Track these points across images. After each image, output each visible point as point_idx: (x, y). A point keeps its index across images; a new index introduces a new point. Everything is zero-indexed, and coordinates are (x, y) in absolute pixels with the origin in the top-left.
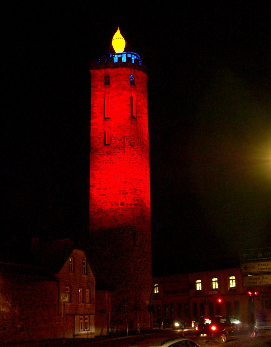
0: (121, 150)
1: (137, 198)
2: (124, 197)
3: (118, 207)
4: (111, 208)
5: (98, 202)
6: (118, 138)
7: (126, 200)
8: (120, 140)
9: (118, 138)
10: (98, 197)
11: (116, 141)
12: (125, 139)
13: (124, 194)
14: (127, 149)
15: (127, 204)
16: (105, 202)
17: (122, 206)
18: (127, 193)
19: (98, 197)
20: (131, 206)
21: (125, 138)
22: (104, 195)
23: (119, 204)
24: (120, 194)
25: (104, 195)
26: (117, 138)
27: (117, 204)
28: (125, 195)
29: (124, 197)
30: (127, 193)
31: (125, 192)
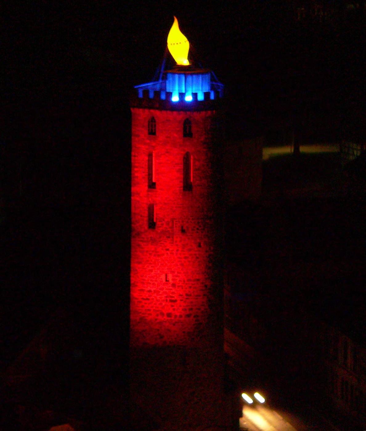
0: (169, 239)
2: (172, 306)
3: (164, 319)
4: (156, 320)
7: (174, 309)
10: (141, 302)
11: (162, 224)
13: (171, 301)
15: (176, 316)
16: (149, 310)
17: (169, 318)
19: (141, 302)
22: (148, 299)
24: (167, 300)
25: (148, 299)
26: (164, 220)
27: (162, 314)
29: (172, 306)
30: (176, 301)
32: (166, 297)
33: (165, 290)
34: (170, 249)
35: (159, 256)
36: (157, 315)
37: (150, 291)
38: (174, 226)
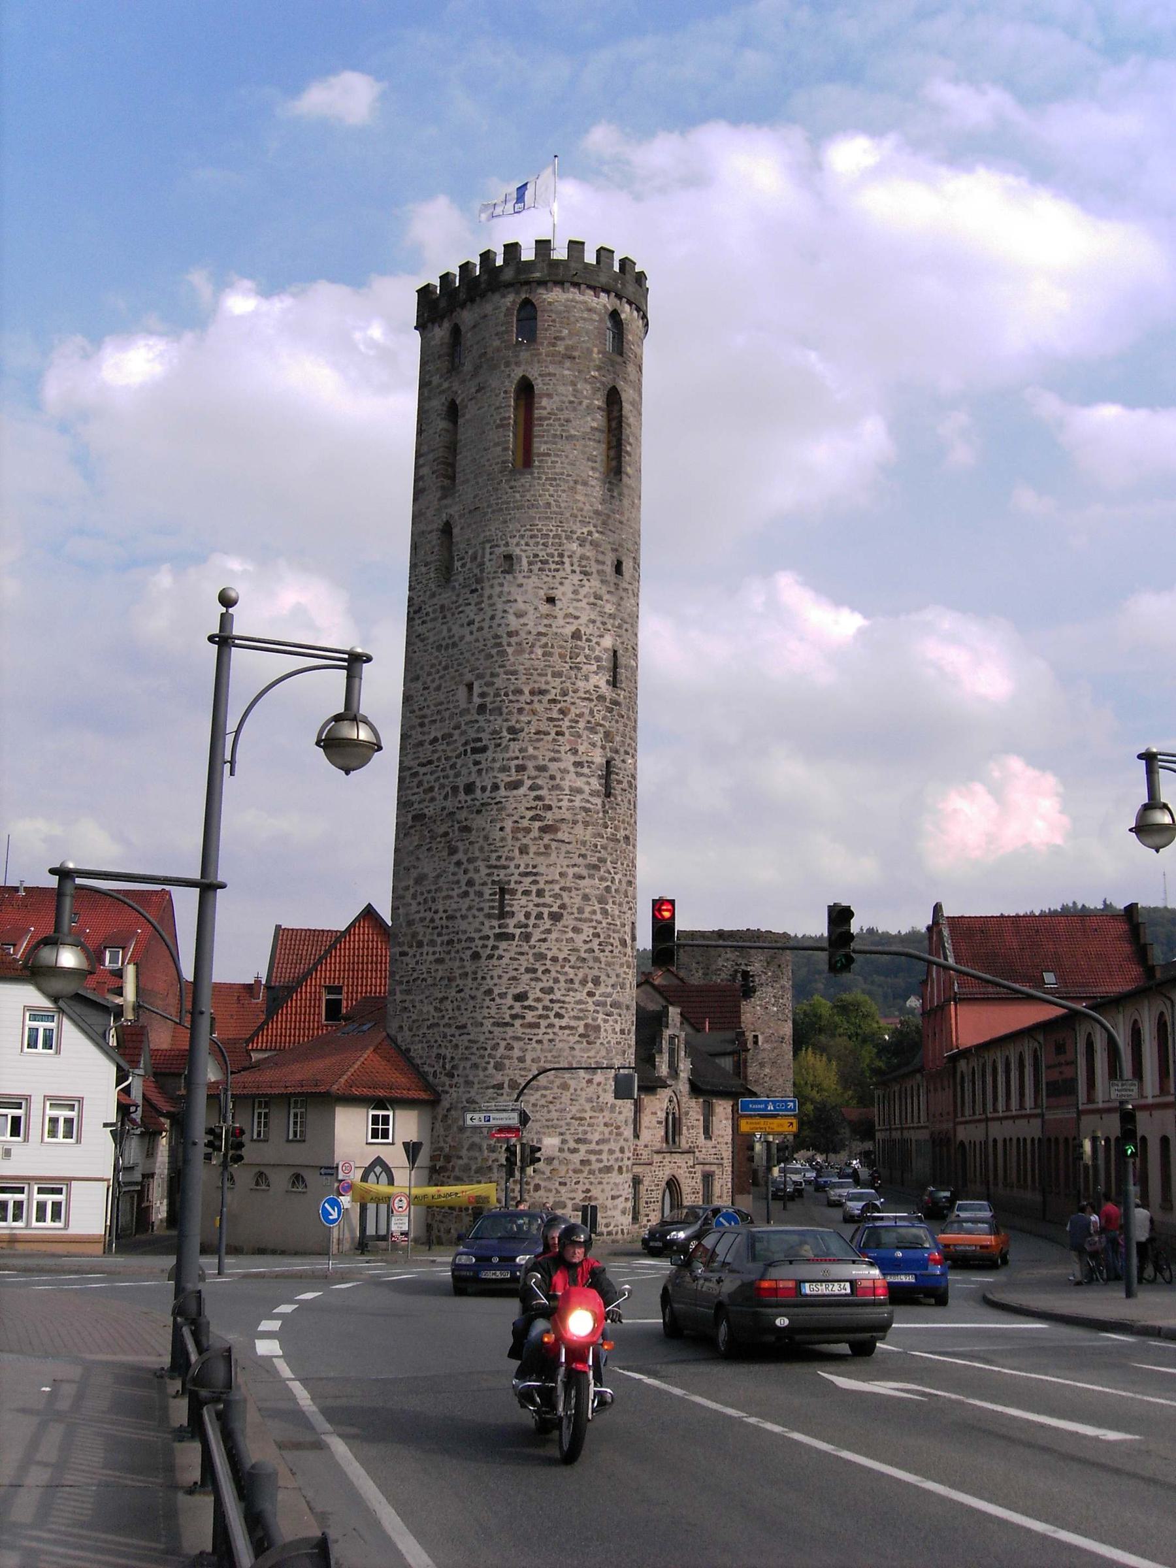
1: (520, 762)
2: (476, 763)
5: (416, 790)
6: (470, 552)
7: (480, 771)
8: (474, 558)
9: (470, 552)
11: (463, 566)
12: (488, 551)
13: (475, 751)
14: (492, 586)
17: (468, 798)
18: (484, 749)
20: (493, 795)
21: (488, 546)
23: (461, 789)
24: (466, 751)
25: (430, 762)
27: (455, 789)
28: (477, 757)
29: (476, 763)
31: (479, 744)
32: (466, 744)
33: (463, 727)
34: (478, 619)
35: (454, 645)
36: (446, 798)
37: (435, 740)
38: (488, 556)
